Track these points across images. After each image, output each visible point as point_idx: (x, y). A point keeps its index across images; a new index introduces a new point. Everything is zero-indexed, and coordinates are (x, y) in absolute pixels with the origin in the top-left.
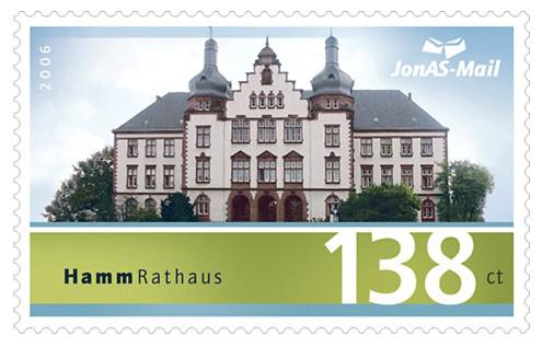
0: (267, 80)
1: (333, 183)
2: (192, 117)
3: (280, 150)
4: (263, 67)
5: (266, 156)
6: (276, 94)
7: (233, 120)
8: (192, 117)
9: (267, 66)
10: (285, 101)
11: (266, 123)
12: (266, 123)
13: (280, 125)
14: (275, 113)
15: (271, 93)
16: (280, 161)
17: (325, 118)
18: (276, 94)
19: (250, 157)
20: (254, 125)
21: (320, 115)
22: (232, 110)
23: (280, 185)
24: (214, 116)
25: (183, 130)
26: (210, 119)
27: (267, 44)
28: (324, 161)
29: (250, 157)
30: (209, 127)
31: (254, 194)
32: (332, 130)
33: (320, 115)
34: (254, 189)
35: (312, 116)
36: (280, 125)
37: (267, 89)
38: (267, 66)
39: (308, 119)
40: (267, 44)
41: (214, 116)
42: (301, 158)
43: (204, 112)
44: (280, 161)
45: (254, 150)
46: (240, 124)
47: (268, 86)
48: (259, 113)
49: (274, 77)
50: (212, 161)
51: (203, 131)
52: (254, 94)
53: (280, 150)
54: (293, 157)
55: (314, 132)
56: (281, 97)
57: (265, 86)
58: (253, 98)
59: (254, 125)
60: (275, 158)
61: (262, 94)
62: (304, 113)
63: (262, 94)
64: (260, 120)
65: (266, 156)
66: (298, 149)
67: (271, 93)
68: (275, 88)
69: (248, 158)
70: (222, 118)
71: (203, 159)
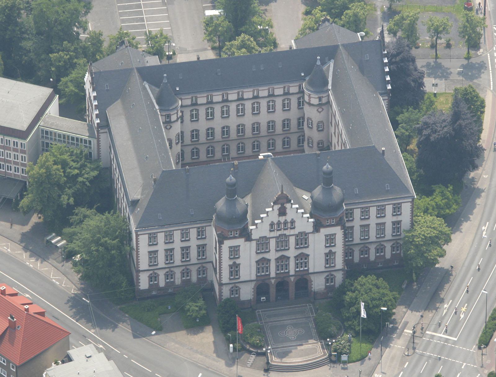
0: (282, 212)
2: (225, 242)
4: (280, 206)
6: (289, 220)
7: (257, 240)
9: (282, 205)
10: (297, 224)
11: (282, 242)
12: (282, 242)
13: (292, 240)
14: (287, 232)
15: (286, 220)
17: (324, 231)
18: (289, 220)
20: (273, 243)
23: (292, 272)
24: (243, 240)
33: (322, 230)
34: (273, 278)
37: (282, 219)
38: (282, 205)
39: (313, 233)
41: (242, 240)
43: (235, 238)
45: (272, 255)
46: (263, 243)
48: (276, 234)
49: (288, 211)
53: (292, 253)
56: (293, 222)
57: (281, 218)
58: (272, 225)
59: (273, 243)
60: (289, 258)
62: (310, 229)
66: (305, 251)
68: (289, 218)
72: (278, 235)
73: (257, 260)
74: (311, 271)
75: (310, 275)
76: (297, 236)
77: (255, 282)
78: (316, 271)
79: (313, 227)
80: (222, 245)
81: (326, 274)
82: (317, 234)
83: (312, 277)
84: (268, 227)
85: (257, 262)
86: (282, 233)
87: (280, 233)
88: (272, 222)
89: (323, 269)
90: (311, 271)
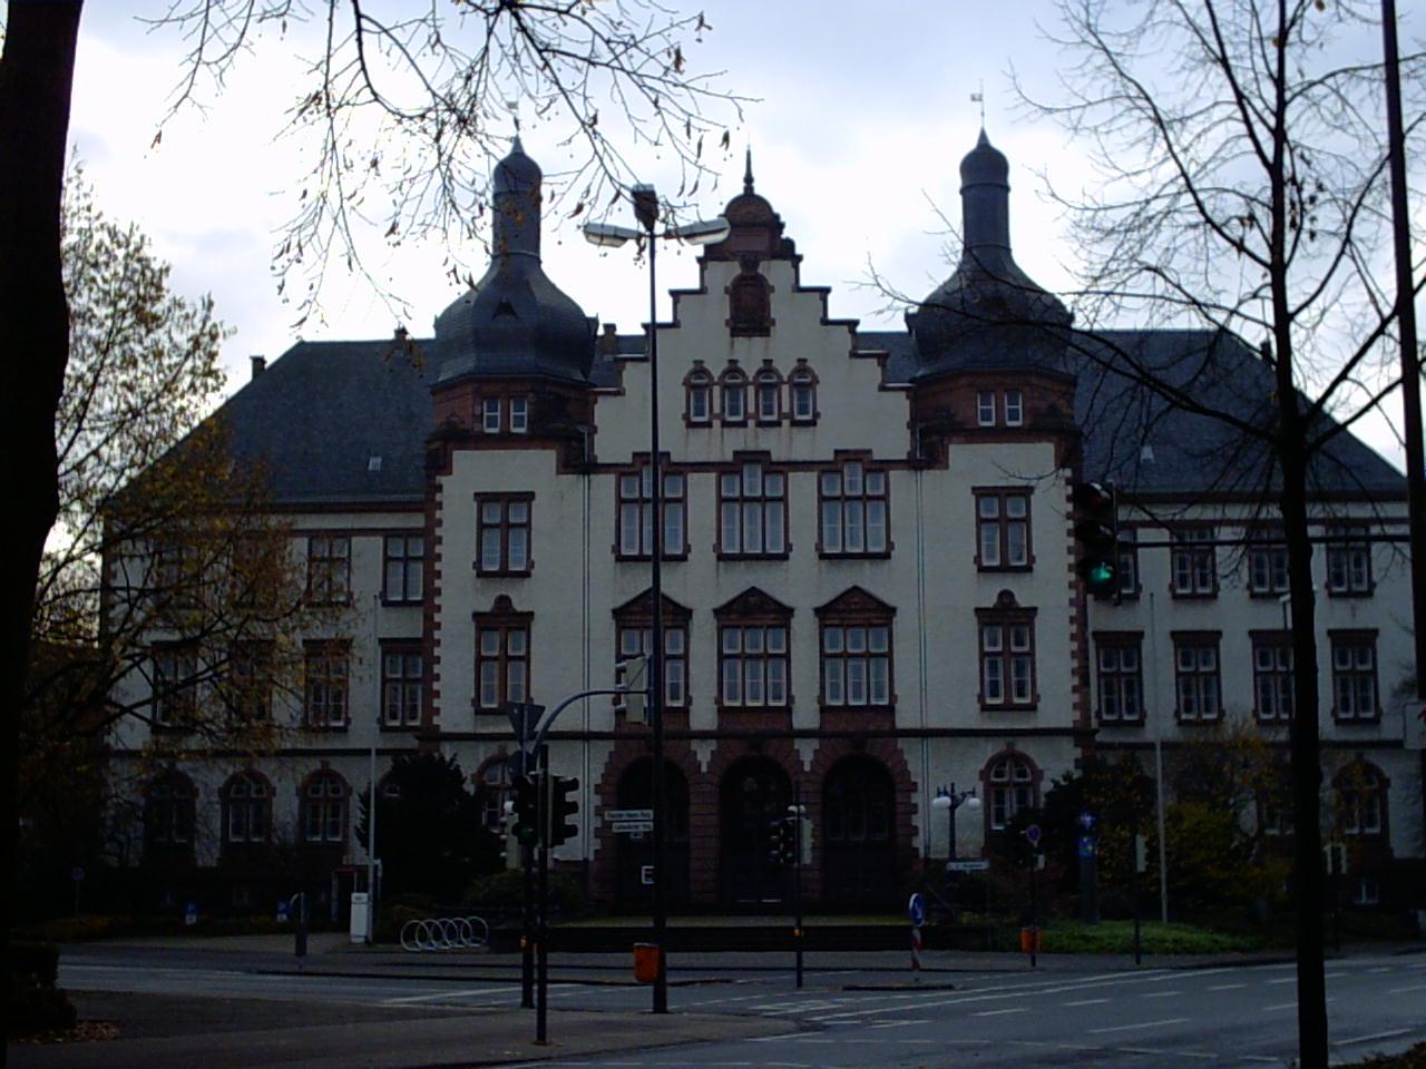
1: (1008, 707)
2: (461, 458)
3: (803, 586)
5: (753, 612)
6: (785, 368)
7: (620, 470)
8: (461, 458)
9: (750, 263)
13: (803, 488)
14: (781, 443)
15: (768, 368)
16: (804, 626)
17: (972, 463)
18: (785, 368)
19: (688, 613)
20: (702, 489)
21: (958, 453)
22: (618, 429)
23: (805, 716)
24: (548, 458)
25: (428, 503)
26: (532, 469)
27: (749, 179)
28: (972, 624)
29: (688, 613)
30: (528, 497)
31: (704, 753)
32: (1002, 509)
33: (958, 453)
34: (704, 736)
35: (927, 455)
36: (803, 488)
37: (751, 354)
39: (913, 464)
40: (749, 179)
41: (548, 458)
42: (886, 613)
43: (506, 440)
44: (804, 626)
47: (758, 341)
48: (719, 445)
50: (536, 628)
51: (505, 512)
52: (699, 370)
53: (803, 586)
54: (859, 614)
55: (934, 515)
56: (804, 383)
57: (741, 342)
58: (698, 380)
59: (702, 489)
60: (786, 613)
61: (733, 369)
62: (894, 440)
63: (733, 369)
64: (722, 469)
65: (753, 612)
67: (768, 368)
68: (783, 348)
69: (682, 616)
70: (578, 462)
71: (505, 624)
72: (729, 457)
73: (621, 601)
74: (906, 718)
75: (901, 743)
76: (826, 469)
77: (610, 745)
78: (934, 722)
79: (911, 425)
80: (442, 480)
81: (991, 749)
82: (928, 475)
83: (915, 759)
84: (674, 400)
85: (618, 613)
86: (751, 447)
87: (740, 447)
88: (699, 370)
89: (971, 718)
90: (906, 718)
